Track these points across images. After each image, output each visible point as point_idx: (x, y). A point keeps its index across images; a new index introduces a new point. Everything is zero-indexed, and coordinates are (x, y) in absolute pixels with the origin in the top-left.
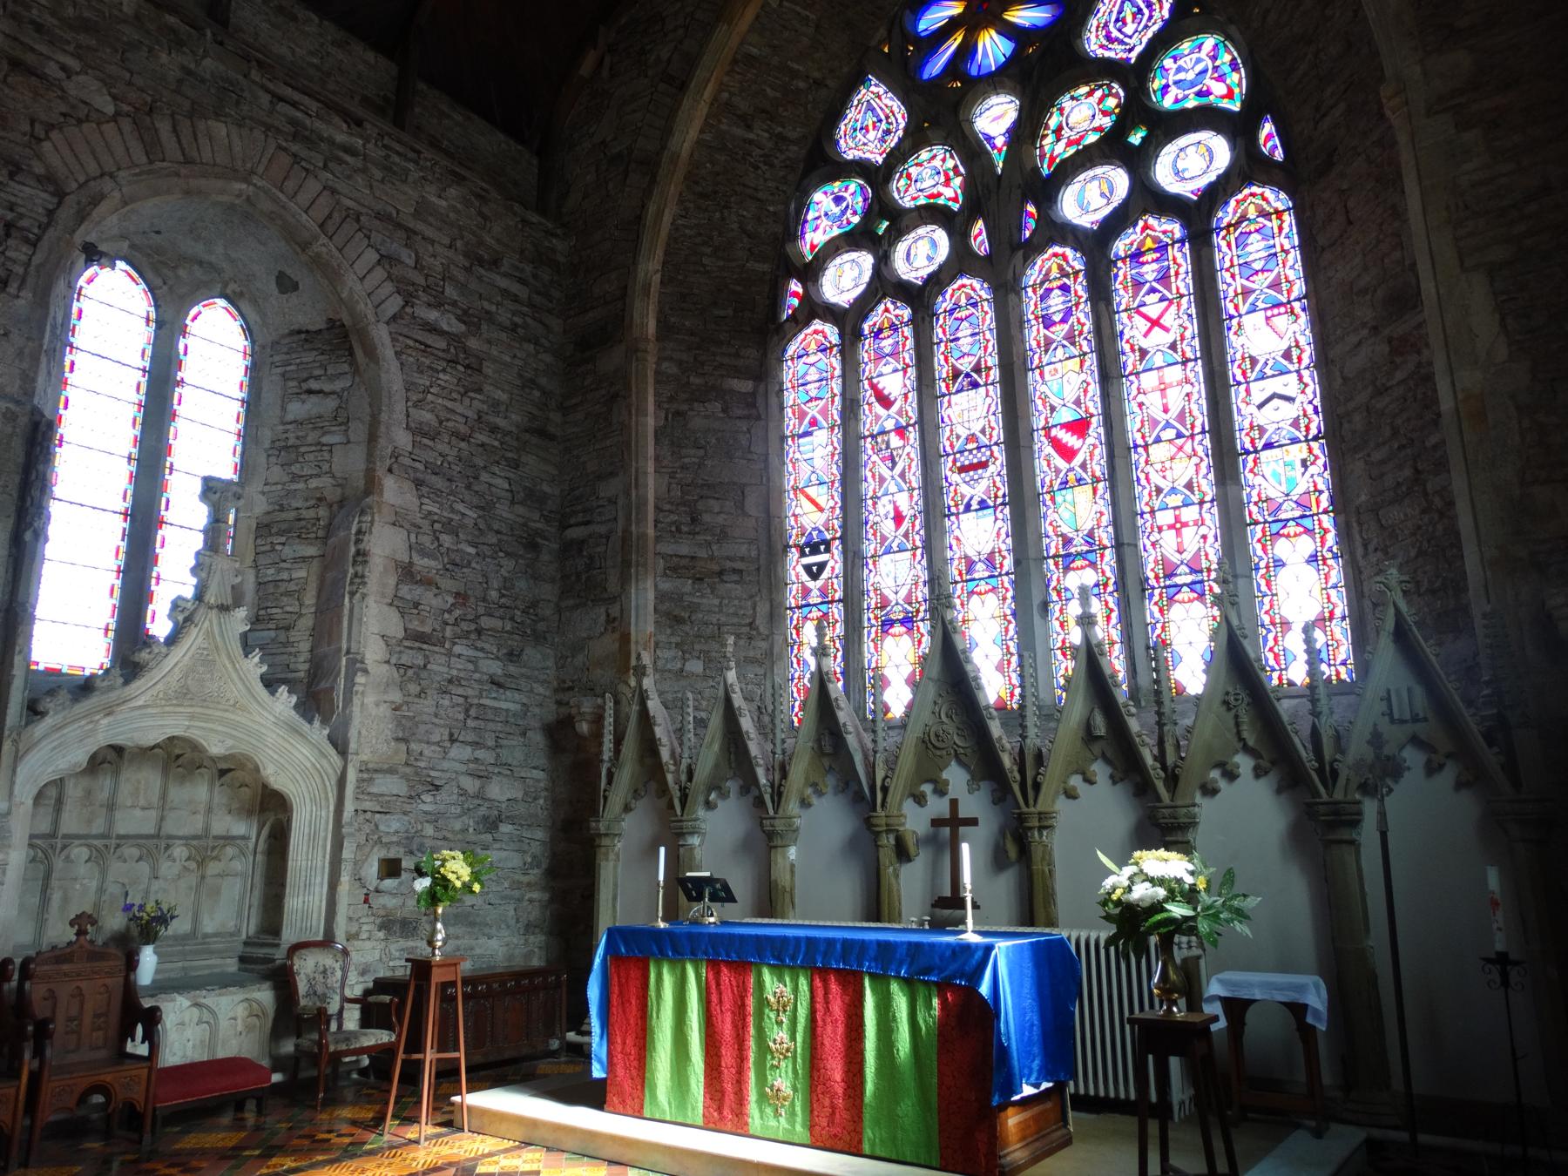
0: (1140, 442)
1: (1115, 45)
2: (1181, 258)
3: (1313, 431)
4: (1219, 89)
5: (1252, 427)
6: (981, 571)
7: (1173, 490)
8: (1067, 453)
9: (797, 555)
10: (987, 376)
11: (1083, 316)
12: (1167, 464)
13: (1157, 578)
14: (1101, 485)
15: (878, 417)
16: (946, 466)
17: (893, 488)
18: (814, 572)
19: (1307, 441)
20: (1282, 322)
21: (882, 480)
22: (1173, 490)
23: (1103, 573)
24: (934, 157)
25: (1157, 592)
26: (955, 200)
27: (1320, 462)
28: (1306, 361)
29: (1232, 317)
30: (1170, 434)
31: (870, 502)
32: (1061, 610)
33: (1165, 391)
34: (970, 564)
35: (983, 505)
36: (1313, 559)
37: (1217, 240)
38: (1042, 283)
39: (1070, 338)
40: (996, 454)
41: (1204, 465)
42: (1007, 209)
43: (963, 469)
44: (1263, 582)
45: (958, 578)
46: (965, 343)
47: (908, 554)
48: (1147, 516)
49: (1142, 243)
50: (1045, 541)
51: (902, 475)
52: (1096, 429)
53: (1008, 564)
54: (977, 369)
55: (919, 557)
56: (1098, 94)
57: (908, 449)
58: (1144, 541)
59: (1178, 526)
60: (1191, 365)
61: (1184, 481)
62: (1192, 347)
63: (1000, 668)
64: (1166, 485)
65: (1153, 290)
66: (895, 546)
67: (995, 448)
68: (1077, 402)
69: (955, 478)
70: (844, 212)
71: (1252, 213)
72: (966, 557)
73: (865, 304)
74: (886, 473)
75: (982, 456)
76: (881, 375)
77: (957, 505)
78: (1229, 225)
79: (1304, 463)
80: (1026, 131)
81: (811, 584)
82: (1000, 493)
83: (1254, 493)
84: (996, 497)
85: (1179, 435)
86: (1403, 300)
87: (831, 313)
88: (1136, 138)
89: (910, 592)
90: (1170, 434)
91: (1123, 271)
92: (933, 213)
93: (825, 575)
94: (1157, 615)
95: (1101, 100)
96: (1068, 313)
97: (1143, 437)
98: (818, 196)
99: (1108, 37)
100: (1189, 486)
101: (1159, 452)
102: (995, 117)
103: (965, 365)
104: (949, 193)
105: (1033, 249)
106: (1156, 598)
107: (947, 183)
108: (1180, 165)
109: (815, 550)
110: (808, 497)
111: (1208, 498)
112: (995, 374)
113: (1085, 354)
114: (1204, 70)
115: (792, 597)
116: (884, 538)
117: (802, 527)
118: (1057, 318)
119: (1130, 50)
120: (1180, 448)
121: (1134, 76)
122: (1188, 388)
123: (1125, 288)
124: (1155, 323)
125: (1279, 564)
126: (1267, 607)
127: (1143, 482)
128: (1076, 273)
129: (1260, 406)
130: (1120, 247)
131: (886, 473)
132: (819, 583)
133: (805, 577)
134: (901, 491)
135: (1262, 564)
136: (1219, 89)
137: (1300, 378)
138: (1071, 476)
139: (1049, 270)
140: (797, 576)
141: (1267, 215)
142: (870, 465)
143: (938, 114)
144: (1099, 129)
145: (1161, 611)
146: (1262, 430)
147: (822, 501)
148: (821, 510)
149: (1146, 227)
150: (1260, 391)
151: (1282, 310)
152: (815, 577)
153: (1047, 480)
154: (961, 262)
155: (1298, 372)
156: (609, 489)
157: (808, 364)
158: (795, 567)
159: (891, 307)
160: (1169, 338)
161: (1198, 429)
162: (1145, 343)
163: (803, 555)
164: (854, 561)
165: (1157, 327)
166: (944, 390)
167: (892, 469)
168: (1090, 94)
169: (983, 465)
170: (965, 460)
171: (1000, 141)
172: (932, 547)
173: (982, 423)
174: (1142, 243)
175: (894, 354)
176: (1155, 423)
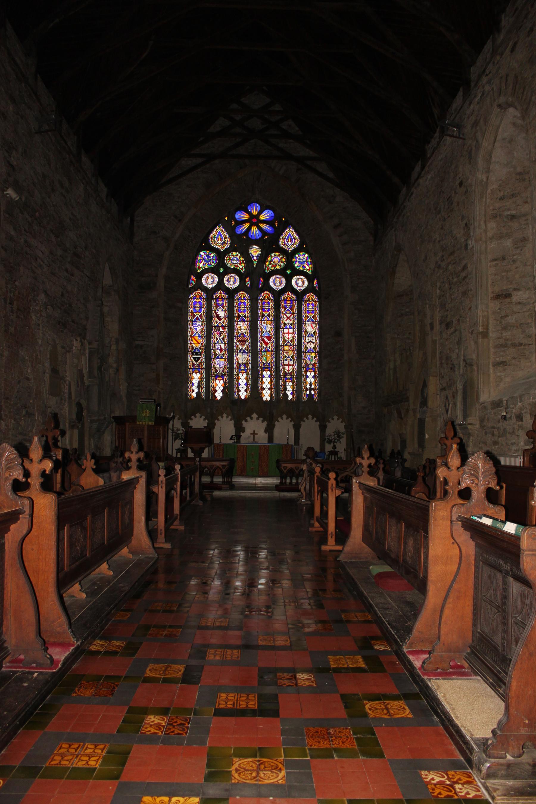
4: (307, 267)
6: (242, 367)
8: (266, 344)
11: (272, 312)
15: (217, 322)
16: (235, 340)
17: (220, 342)
18: (197, 360)
20: (314, 326)
21: (217, 339)
22: (289, 357)
24: (237, 255)
26: (242, 269)
30: (289, 344)
33: (288, 335)
35: (244, 352)
36: (313, 377)
37: (303, 303)
39: (269, 315)
42: (255, 278)
43: (239, 341)
46: (242, 308)
47: (223, 360)
49: (287, 298)
51: (223, 339)
52: (273, 339)
53: (250, 366)
54: (245, 316)
56: (281, 256)
59: (289, 365)
62: (295, 326)
63: (246, 391)
65: (288, 310)
68: (269, 332)
69: (238, 343)
70: (210, 260)
74: (218, 337)
76: (218, 310)
80: (263, 259)
87: (205, 289)
88: (289, 272)
90: (289, 344)
92: (235, 271)
93: (200, 361)
95: (281, 258)
96: (269, 310)
98: (202, 253)
99: (284, 242)
100: (292, 357)
101: (286, 348)
102: (255, 251)
104: (241, 267)
105: (262, 290)
107: (240, 264)
108: (298, 282)
109: (197, 354)
110: (195, 339)
112: (249, 319)
115: (189, 365)
116: (217, 354)
118: (266, 310)
120: (291, 348)
121: (289, 256)
124: (288, 318)
125: (307, 377)
128: (272, 300)
129: (308, 343)
131: (218, 337)
133: (193, 361)
134: (222, 343)
136: (307, 267)
141: (314, 301)
143: (241, 243)
144: (280, 266)
147: (199, 341)
148: (199, 344)
149: (288, 294)
152: (197, 361)
154: (242, 287)
157: (195, 302)
158: (191, 358)
160: (291, 322)
163: (193, 355)
164: (208, 359)
165: (288, 319)
168: (279, 256)
169: (245, 342)
170: (240, 339)
171: (255, 258)
172: (231, 359)
173: (245, 331)
176: (286, 341)
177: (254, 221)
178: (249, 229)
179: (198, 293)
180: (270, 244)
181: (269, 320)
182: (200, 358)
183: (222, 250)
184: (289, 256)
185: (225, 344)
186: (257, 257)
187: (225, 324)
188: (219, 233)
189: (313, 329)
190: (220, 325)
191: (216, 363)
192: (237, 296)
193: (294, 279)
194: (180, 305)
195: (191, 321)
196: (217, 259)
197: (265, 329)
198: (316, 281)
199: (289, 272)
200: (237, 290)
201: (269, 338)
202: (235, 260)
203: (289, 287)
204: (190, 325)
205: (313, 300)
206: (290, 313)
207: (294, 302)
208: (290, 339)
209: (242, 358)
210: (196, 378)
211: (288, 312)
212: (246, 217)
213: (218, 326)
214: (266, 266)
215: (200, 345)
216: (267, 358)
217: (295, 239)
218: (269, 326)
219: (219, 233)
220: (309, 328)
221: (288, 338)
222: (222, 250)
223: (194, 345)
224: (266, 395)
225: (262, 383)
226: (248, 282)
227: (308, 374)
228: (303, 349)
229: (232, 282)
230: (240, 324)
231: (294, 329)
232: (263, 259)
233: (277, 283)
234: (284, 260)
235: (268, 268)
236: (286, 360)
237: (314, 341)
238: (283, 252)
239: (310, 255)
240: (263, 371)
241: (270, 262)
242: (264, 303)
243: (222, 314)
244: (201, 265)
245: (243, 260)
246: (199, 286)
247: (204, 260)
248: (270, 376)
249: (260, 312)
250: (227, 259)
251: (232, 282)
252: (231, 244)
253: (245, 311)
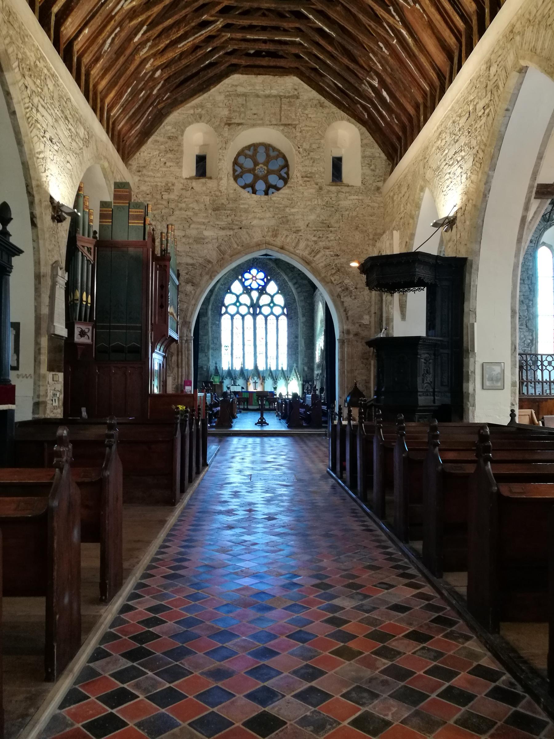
80: (258, 299)
86: (297, 337)
92: (245, 305)
102: (255, 294)
105: (258, 314)
143: (247, 290)
154: (249, 313)
156: (205, 337)
157: (225, 321)
158: (223, 348)
177: (254, 278)
180: (262, 291)
194: (217, 323)
202: (245, 299)
203: (272, 313)
212: (250, 276)
226: (251, 310)
229: (243, 310)
232: (258, 299)
233: (266, 310)
246: (226, 312)
247: (229, 299)
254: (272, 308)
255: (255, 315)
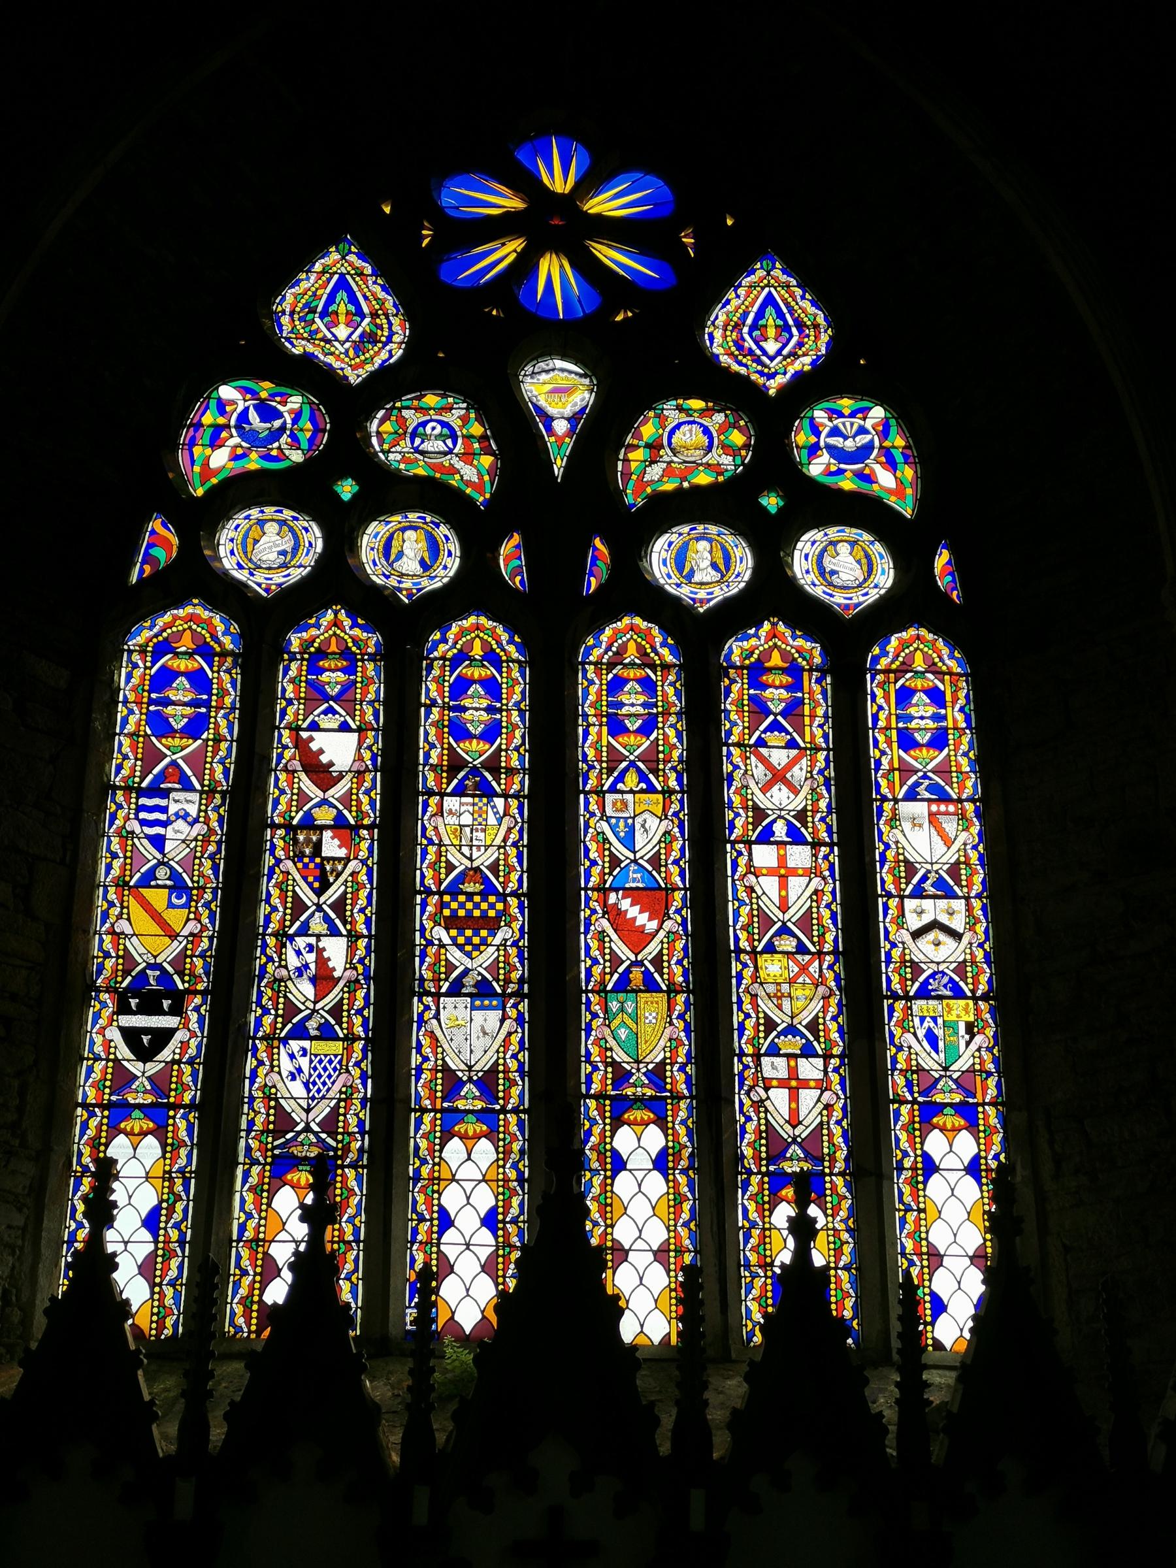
0: (744, 944)
1: (747, 360)
2: (817, 697)
3: (982, 988)
4: (886, 479)
5: (903, 962)
6: (470, 1099)
7: (791, 1030)
9: (111, 1007)
10: (509, 784)
12: (785, 988)
13: (757, 1158)
14: (681, 998)
15: (303, 798)
17: (318, 925)
19: (975, 999)
20: (950, 826)
21: (299, 906)
23: (676, 1135)
25: (755, 1180)
27: (990, 1032)
28: (977, 888)
29: (884, 799)
30: (788, 944)
31: (271, 941)
32: (604, 1185)
33: (782, 881)
34: (453, 1085)
35: (483, 990)
38: (611, 666)
39: (652, 759)
40: (514, 910)
41: (834, 1001)
43: (451, 923)
44: (907, 1190)
45: (427, 1103)
46: (476, 716)
47: (337, 1047)
48: (748, 1060)
49: (767, 654)
50: (586, 1069)
51: (339, 906)
53: (517, 1093)
55: (357, 1055)
57: (353, 865)
58: (741, 1098)
59: (794, 1084)
60: (824, 850)
61: (806, 1017)
64: (781, 1020)
65: (775, 727)
66: (312, 1025)
67: (513, 902)
68: (655, 861)
69: (440, 933)
70: (276, 435)
71: (919, 663)
72: (446, 1069)
73: (299, 602)
74: (307, 895)
75: (490, 907)
76: (314, 727)
77: (437, 980)
78: (887, 671)
79: (970, 1027)
80: (603, 431)
81: (136, 1068)
82: (515, 976)
83: (901, 1057)
84: (508, 981)
85: (801, 949)
89: (335, 1111)
90: (788, 944)
91: (738, 688)
93: (166, 1054)
94: (753, 1215)
97: (750, 940)
99: (739, 345)
100: (813, 1026)
102: (557, 391)
103: (474, 751)
105: (606, 608)
106: (753, 1189)
107: (468, 456)
109: (150, 1006)
111: (836, 1051)
113: (672, 792)
114: (856, 442)
116: (291, 1009)
117: (127, 955)
118: (633, 725)
119: (771, 376)
120: (804, 969)
121: (771, 418)
122: (816, 882)
123: (740, 712)
124: (778, 776)
125: (930, 1167)
126: (909, 1227)
127: (747, 1007)
128: (666, 667)
129: (917, 934)
130: (736, 649)
131: (307, 895)
132: (152, 1068)
133: (124, 1052)
134: (334, 932)
135: (907, 1163)
137: (969, 908)
138: (636, 975)
139: (623, 649)
140: (107, 1044)
141: (938, 673)
142: (278, 877)
143: (467, 346)
144: (717, 469)
145: (760, 1210)
146: (916, 969)
147: (175, 918)
148: (173, 936)
149: (773, 635)
150: (920, 911)
151: (951, 808)
152: (144, 1054)
153: (597, 970)
154: (474, 589)
155: (967, 898)
159: (347, 623)
160: (798, 803)
161: (828, 947)
162: (762, 801)
163: (123, 1008)
165: (780, 779)
166: (431, 783)
167: (319, 893)
171: (561, 427)
174: (767, 654)
175: (346, 696)
176: (767, 922)
177: (555, 225)
178: (525, 266)
179: (192, 618)
181: (651, 789)
182: (169, 1033)
183: (354, 378)
184: (771, 418)
185: (353, 937)
186: (573, 419)
187: (361, 814)
188: (342, 284)
189: (948, 843)
190: (324, 816)
191: (286, 1065)
192: (444, 644)
193: (808, 544)
195: (128, 789)
196: (317, 430)
197: (629, 841)
198: (942, 559)
199: (771, 502)
200: (440, 608)
201: (654, 898)
202: (433, 436)
203: (773, 594)
204: (122, 814)
205: (932, 668)
206: (791, 744)
207: (810, 682)
208: (795, 912)
209: (470, 1035)
210: (139, 1172)
211: (774, 738)
212: (503, 201)
213: (308, 823)
214: (627, 475)
215: (176, 947)
216: (643, 1032)
217: (800, 325)
218: (652, 823)
219: (342, 284)
220: (928, 836)
221: (784, 907)
222: (354, 378)
223: (135, 947)
224: (646, 1312)
225: (610, 1207)
226: (509, 557)
227: (935, 1144)
228: (892, 977)
230: (459, 810)
231: (816, 845)
234: (737, 438)
235: (641, 484)
236: (774, 1051)
237: (958, 923)
238: (730, 392)
239: (904, 412)
240: (617, 1122)
241: (654, 447)
242: (617, 685)
243: (338, 749)
244: (219, 458)
245: (483, 438)
248: (661, 1163)
249: (593, 739)
250: (379, 427)
251: (407, 555)
252: (411, 346)
253: (491, 733)
254: (772, 543)
255: (552, 631)
